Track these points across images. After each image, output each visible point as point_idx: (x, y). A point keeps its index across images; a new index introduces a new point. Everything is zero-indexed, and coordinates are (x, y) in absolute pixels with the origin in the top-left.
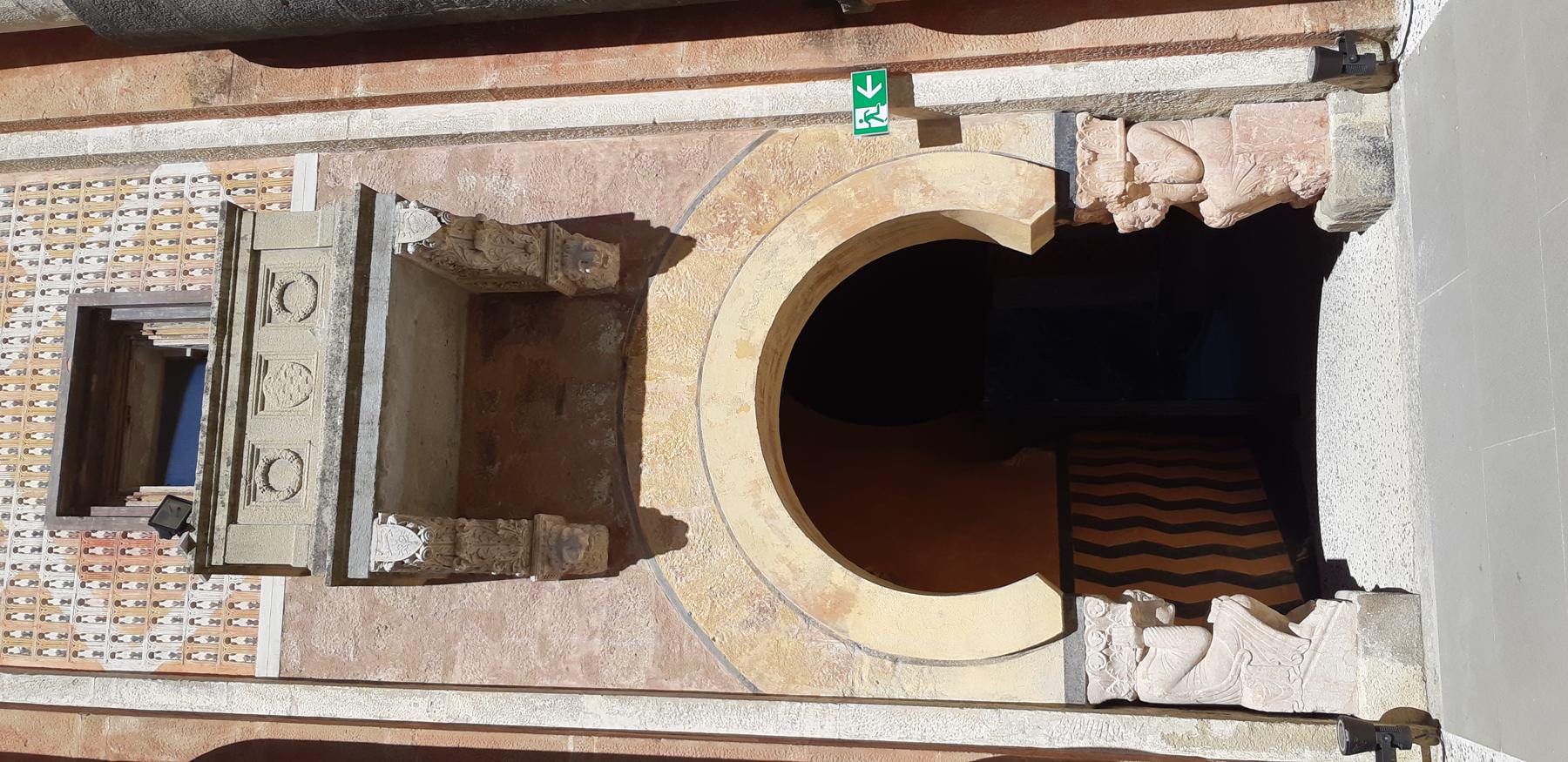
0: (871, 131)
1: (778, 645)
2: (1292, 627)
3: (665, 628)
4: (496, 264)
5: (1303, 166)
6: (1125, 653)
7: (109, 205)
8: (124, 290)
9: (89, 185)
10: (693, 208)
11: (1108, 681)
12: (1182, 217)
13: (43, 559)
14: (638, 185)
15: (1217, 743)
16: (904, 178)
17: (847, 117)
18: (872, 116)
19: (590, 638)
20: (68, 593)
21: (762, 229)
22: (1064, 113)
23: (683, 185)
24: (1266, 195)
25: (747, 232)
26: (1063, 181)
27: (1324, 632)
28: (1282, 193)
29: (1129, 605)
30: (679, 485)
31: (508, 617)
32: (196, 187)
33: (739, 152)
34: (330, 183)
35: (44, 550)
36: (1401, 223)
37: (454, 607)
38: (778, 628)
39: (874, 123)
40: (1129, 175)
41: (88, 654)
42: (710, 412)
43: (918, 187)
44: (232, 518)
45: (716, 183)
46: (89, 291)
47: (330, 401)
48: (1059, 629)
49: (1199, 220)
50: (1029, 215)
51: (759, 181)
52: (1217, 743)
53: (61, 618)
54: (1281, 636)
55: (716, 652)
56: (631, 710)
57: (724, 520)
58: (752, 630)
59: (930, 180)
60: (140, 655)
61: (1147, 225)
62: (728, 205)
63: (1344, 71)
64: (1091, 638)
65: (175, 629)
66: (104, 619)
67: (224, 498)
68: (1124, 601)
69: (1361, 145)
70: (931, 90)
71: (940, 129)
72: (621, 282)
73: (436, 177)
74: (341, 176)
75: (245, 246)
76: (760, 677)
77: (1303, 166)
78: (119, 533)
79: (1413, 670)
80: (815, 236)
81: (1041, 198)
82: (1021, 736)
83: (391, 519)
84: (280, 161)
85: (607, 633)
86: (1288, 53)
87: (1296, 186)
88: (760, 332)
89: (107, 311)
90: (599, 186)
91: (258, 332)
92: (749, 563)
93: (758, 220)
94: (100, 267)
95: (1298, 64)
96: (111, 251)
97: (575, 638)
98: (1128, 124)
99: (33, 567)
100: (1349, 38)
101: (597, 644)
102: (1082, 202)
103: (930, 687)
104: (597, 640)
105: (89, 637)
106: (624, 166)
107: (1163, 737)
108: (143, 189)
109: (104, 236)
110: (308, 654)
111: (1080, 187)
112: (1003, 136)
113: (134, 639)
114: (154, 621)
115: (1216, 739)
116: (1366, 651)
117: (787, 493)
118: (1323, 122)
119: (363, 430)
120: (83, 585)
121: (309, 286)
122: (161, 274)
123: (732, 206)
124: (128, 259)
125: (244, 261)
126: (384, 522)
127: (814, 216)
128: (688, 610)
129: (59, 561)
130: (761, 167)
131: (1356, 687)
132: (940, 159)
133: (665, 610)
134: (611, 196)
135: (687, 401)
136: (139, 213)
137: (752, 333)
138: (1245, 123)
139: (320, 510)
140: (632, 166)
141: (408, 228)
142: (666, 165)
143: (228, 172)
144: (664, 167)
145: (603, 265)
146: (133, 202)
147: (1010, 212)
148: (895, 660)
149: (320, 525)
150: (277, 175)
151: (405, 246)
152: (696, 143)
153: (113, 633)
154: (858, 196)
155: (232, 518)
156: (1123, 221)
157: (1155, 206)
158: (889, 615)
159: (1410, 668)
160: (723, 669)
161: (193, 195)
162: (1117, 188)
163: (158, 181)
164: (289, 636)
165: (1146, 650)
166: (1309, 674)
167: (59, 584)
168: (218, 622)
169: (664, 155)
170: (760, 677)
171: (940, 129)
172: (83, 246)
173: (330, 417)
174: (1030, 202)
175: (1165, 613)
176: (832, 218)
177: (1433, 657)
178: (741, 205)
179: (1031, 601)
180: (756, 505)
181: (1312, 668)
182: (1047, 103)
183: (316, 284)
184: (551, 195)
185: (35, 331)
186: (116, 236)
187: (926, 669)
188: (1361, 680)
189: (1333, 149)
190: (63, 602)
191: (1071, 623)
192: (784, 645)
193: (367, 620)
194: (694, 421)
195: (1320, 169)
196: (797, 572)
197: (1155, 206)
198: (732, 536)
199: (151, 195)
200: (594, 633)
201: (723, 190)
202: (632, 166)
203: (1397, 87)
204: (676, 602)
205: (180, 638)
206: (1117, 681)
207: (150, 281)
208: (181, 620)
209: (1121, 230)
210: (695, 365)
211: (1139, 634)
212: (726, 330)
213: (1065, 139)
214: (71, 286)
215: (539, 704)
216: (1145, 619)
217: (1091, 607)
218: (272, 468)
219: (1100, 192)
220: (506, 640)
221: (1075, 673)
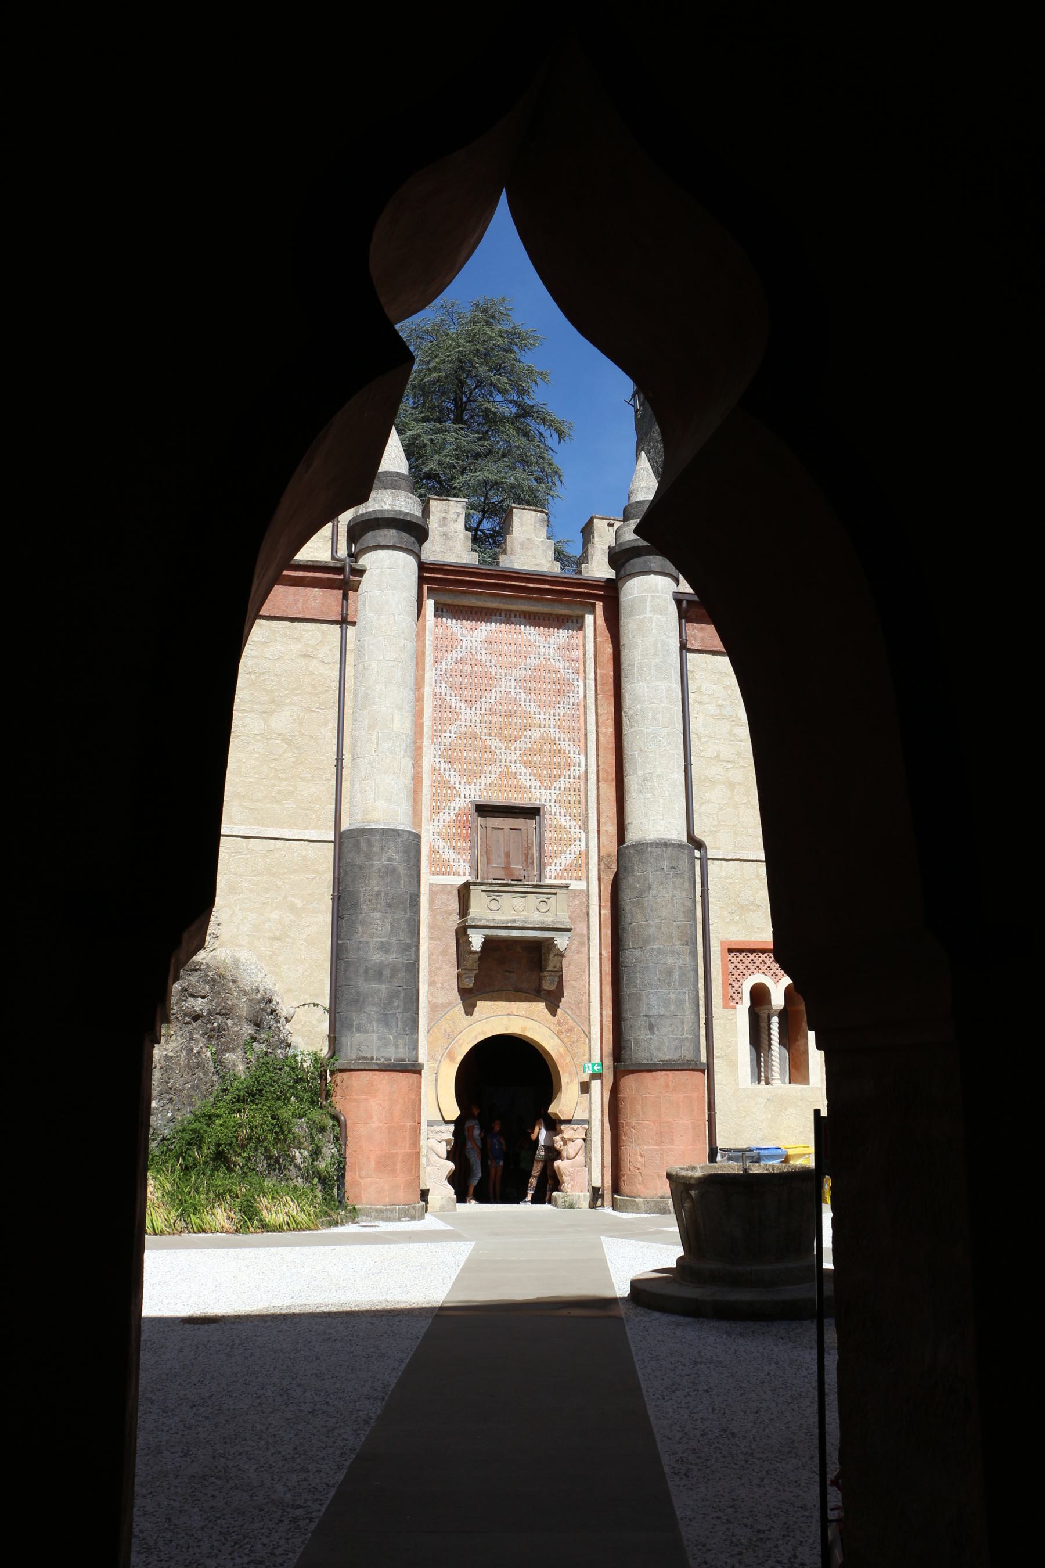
0: (584, 1068)
3: (443, 1006)
17: (590, 1061)
21: (558, 1034)
22: (587, 1122)
26: (569, 1122)
40: (569, 1140)
47: (515, 921)
48: (447, 1119)
49: (556, 1159)
62: (566, 1023)
64: (444, 1127)
67: (489, 888)
70: (596, 1085)
71: (585, 1088)
75: (558, 891)
84: (584, 876)
85: (442, 988)
95: (597, 1183)
98: (584, 1140)
100: (602, 1196)
102: (562, 1127)
125: (553, 891)
127: (562, 1050)
129: (462, 805)
132: (576, 1088)
141: (561, 942)
144: (578, 1003)
145: (548, 985)
146: (573, 823)
147: (560, 1107)
149: (481, 920)
152: (585, 1013)
162: (566, 1135)
171: (585, 1088)
173: (510, 921)
176: (561, 1055)
179: (453, 1112)
182: (590, 1117)
185: (533, 790)
186: (563, 818)
191: (447, 1122)
193: (446, 912)
196: (460, 1046)
201: (571, 1022)
212: (530, 1024)
214: (548, 804)
216: (448, 1142)
217: (452, 1128)
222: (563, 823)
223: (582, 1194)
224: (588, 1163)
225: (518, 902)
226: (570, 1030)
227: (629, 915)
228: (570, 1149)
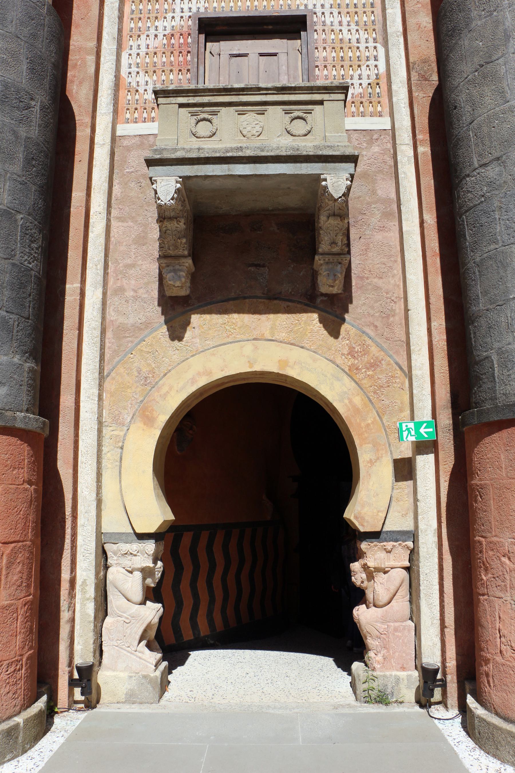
0: (399, 431)
1: (128, 387)
2: (144, 642)
3: (138, 328)
4: (324, 227)
5: (379, 658)
6: (128, 562)
7: (362, 24)
8: (316, 37)
9: (373, 12)
10: (364, 332)
11: (115, 553)
12: (359, 596)
13: (178, 14)
14: (376, 301)
15: (83, 605)
16: (378, 450)
17: (412, 419)
18: (409, 432)
19: (133, 290)
20: (160, 29)
21: (351, 373)
23: (376, 327)
24: (366, 639)
25: (350, 363)
26: (375, 535)
27: (140, 658)
28: (368, 648)
29: (152, 565)
30: (210, 332)
31: (144, 247)
32: (372, 67)
33: (395, 357)
34: (375, 136)
35: (182, 14)
36: (349, 706)
37: (150, 219)
38: (137, 387)
39: (405, 434)
40: (378, 570)
41: (131, 43)
42: (248, 348)
43: (373, 458)
44: (181, 106)
45: (378, 345)
46: (315, 19)
47: (241, 149)
48: (138, 531)
49: (357, 604)
50: (356, 518)
51: (379, 369)
52: (83, 605)
53: (149, 27)
54: (138, 637)
55: (125, 355)
56: (95, 313)
57: (192, 356)
58: (136, 374)
59: (378, 464)
60: (130, 68)
61: (353, 578)
62: (366, 352)
63: (425, 682)
64: (135, 546)
65: (142, 83)
66: (148, 48)
68: (155, 562)
69: (390, 687)
70: (425, 464)
71: (404, 470)
72: (322, 295)
73: (379, 192)
74: (379, 142)
75: (326, 97)
76: (114, 379)
77: (379, 658)
78: (190, 49)
79: (123, 698)
80: (347, 401)
81: (365, 524)
82: (84, 511)
83: (179, 185)
84: (387, 110)
86: (439, 653)
87: (371, 654)
88: (293, 373)
89: (305, 30)
90: (376, 280)
91: (279, 108)
92: (170, 371)
93: (357, 369)
94: (328, 22)
95: (432, 657)
96: (337, 28)
97: (133, 282)
98: (408, 569)
99: (174, 9)
101: (130, 294)
102: (364, 546)
103: (109, 466)
104: (132, 293)
105: (139, 42)
106: (387, 293)
107: (85, 580)
108: (371, 40)
109: (345, 23)
110: (128, 149)
111: (372, 544)
112: (401, 503)
113: (138, 64)
114: (147, 72)
115: (85, 605)
116: (131, 677)
117: (210, 389)
118: (403, 669)
119: (225, 166)
120: (164, 35)
121: (304, 132)
122: (325, 54)
123: (365, 354)
124: (333, 36)
125: (317, 97)
126: (177, 182)
127: (358, 400)
128: (146, 339)
130: (386, 370)
131: (114, 671)
132: (387, 470)
133: (147, 327)
134: (370, 287)
135: (256, 334)
136: (357, 40)
137: (292, 368)
138: (404, 629)
139: (184, 149)
140: (387, 298)
141: (335, 181)
142: (388, 317)
143: (380, 83)
144: (387, 316)
145: (328, 285)
146: (363, 36)
148: (122, 448)
149: (175, 150)
150: (379, 109)
151: (325, 180)
152: (400, 334)
153: (141, 53)
154: (368, 425)
155: (181, 106)
156: (355, 566)
157: (362, 582)
158: (142, 446)
159: (124, 696)
160: (117, 359)
161: (368, 66)
162: (371, 563)
163: (375, 48)
164: (137, 138)
165: (131, 572)
166: (120, 650)
167: (165, 24)
168: (145, 103)
169: (393, 316)
170: (114, 379)
171: (404, 470)
172: (339, 13)
173: (232, 149)
174: (363, 518)
175: (151, 583)
176: (357, 411)
177: (126, 709)
178: (366, 359)
180: (199, 374)
181: (123, 651)
182: (416, 527)
183: (306, 135)
184: (370, 254)
187: (118, 464)
188: (118, 673)
189: (388, 673)
190: (157, 27)
191: (142, 537)
192: (129, 390)
194: (245, 338)
195: (377, 666)
196: (164, 396)
197: (362, 582)
198: (184, 361)
199: (367, 45)
200: (135, 291)
201: (374, 349)
202: (387, 298)
203: (417, 708)
204: (151, 333)
205: (138, 86)
206: (115, 558)
207: (321, 49)
208: (147, 85)
209: (351, 564)
210: (276, 337)
211: (138, 570)
213: (398, 536)
215: (99, 267)
216: (146, 573)
217: (150, 546)
218: (208, 123)
219: (369, 554)
220: (133, 247)
221: (117, 538)
222: (346, 36)
223: (403, 674)
224: (415, 615)
225: (250, 121)
226: (374, 365)
227: (468, 108)
228: (379, 588)
